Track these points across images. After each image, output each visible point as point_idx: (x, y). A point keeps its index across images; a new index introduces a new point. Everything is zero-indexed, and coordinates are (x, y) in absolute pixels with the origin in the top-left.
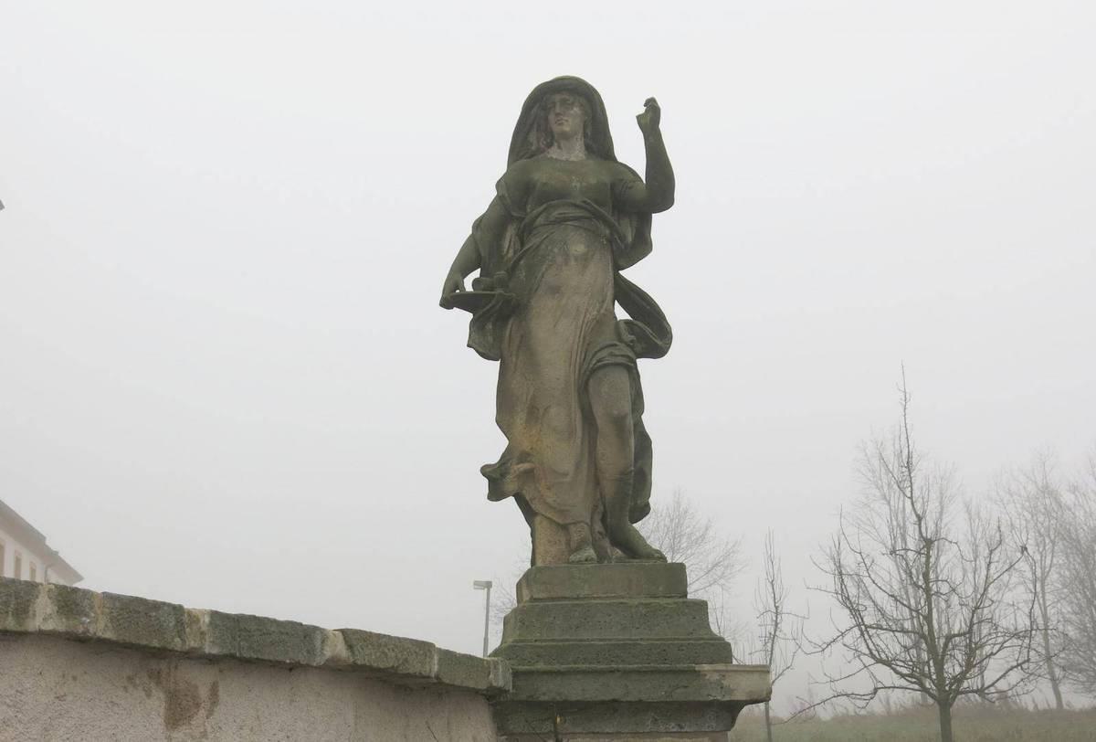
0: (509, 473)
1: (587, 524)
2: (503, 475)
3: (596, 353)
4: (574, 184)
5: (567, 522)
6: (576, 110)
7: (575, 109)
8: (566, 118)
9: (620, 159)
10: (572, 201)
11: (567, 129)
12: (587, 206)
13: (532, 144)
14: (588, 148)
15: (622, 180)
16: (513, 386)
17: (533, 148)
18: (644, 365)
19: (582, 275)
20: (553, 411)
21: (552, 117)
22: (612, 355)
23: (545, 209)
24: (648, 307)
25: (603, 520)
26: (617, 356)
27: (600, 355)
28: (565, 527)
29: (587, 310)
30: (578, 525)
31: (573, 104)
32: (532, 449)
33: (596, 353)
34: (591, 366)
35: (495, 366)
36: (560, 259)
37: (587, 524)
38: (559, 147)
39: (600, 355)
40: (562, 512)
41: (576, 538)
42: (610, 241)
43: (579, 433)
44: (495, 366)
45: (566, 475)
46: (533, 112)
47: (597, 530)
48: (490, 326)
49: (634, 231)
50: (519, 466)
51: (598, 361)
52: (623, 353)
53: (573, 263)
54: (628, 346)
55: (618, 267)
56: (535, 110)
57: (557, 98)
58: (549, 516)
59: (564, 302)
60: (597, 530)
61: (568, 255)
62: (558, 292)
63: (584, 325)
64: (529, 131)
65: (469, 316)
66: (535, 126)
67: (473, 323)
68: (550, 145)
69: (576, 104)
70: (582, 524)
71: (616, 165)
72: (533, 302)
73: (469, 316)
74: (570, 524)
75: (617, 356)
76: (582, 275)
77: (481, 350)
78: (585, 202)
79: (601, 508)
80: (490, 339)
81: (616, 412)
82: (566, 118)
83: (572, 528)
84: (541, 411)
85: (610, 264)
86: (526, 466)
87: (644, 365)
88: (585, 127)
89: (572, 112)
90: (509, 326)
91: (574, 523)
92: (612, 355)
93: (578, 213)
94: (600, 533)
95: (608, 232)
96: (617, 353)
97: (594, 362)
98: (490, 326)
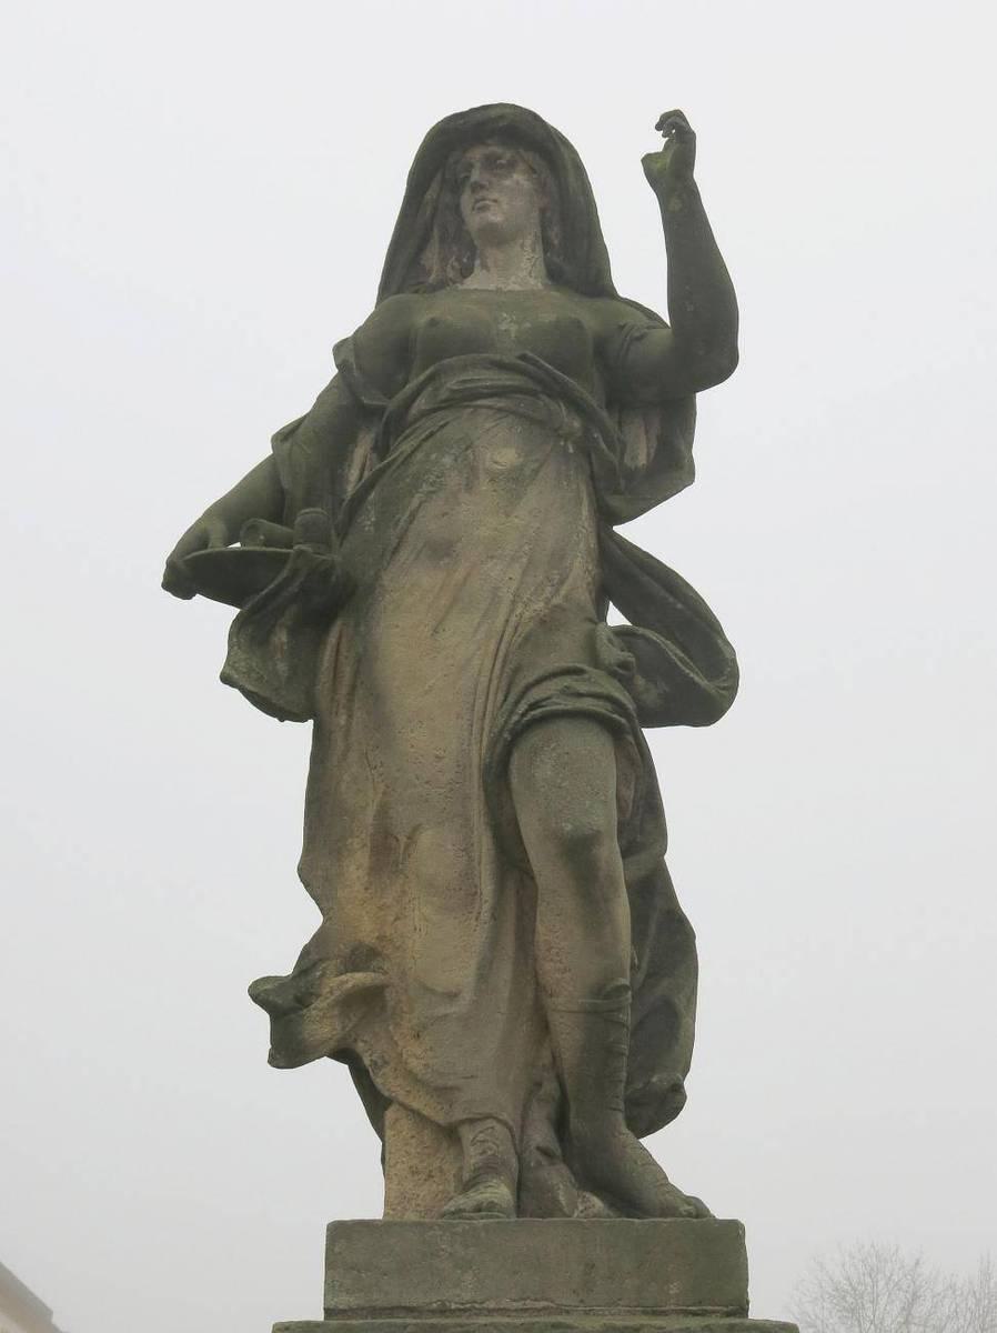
0: (318, 996)
1: (505, 1124)
3: (528, 688)
4: (503, 327)
5: (458, 1115)
6: (519, 178)
7: (515, 176)
8: (495, 195)
9: (622, 292)
10: (491, 356)
11: (495, 217)
12: (531, 367)
13: (429, 273)
14: (555, 276)
15: (622, 327)
16: (343, 787)
17: (432, 279)
19: (508, 515)
20: (426, 838)
21: (467, 200)
23: (431, 378)
24: (679, 606)
26: (580, 695)
27: (535, 695)
28: (450, 1134)
29: (517, 595)
30: (480, 1126)
31: (511, 165)
32: (381, 938)
33: (528, 688)
34: (515, 718)
35: (301, 734)
36: (454, 480)
37: (505, 1124)
38: (484, 266)
39: (535, 695)
40: (443, 1092)
41: (473, 1157)
42: (586, 450)
43: (487, 887)
44: (301, 734)
45: (452, 996)
46: (428, 196)
47: (533, 1145)
48: (281, 637)
49: (654, 444)
50: (343, 977)
51: (533, 706)
52: (598, 690)
53: (484, 485)
54: (613, 674)
55: (607, 516)
56: (430, 195)
57: (477, 154)
58: (415, 1105)
59: (459, 576)
60: (533, 1145)
61: (473, 469)
62: (448, 555)
63: (510, 630)
64: (424, 242)
65: (228, 613)
66: (436, 233)
67: (239, 626)
68: (466, 272)
69: (521, 166)
70: (490, 1123)
71: (615, 302)
72: (386, 579)
73: (228, 613)
74: (463, 1122)
75: (580, 695)
76: (508, 515)
77: (250, 687)
78: (523, 357)
79: (550, 1087)
80: (282, 667)
81: (569, 827)
83: (467, 1134)
84: (403, 840)
85: (586, 502)
88: (544, 226)
89: (507, 182)
90: (332, 639)
91: (471, 1121)
93: (506, 379)
94: (545, 1152)
95: (577, 424)
96: (583, 688)
97: (522, 707)
98: (281, 637)
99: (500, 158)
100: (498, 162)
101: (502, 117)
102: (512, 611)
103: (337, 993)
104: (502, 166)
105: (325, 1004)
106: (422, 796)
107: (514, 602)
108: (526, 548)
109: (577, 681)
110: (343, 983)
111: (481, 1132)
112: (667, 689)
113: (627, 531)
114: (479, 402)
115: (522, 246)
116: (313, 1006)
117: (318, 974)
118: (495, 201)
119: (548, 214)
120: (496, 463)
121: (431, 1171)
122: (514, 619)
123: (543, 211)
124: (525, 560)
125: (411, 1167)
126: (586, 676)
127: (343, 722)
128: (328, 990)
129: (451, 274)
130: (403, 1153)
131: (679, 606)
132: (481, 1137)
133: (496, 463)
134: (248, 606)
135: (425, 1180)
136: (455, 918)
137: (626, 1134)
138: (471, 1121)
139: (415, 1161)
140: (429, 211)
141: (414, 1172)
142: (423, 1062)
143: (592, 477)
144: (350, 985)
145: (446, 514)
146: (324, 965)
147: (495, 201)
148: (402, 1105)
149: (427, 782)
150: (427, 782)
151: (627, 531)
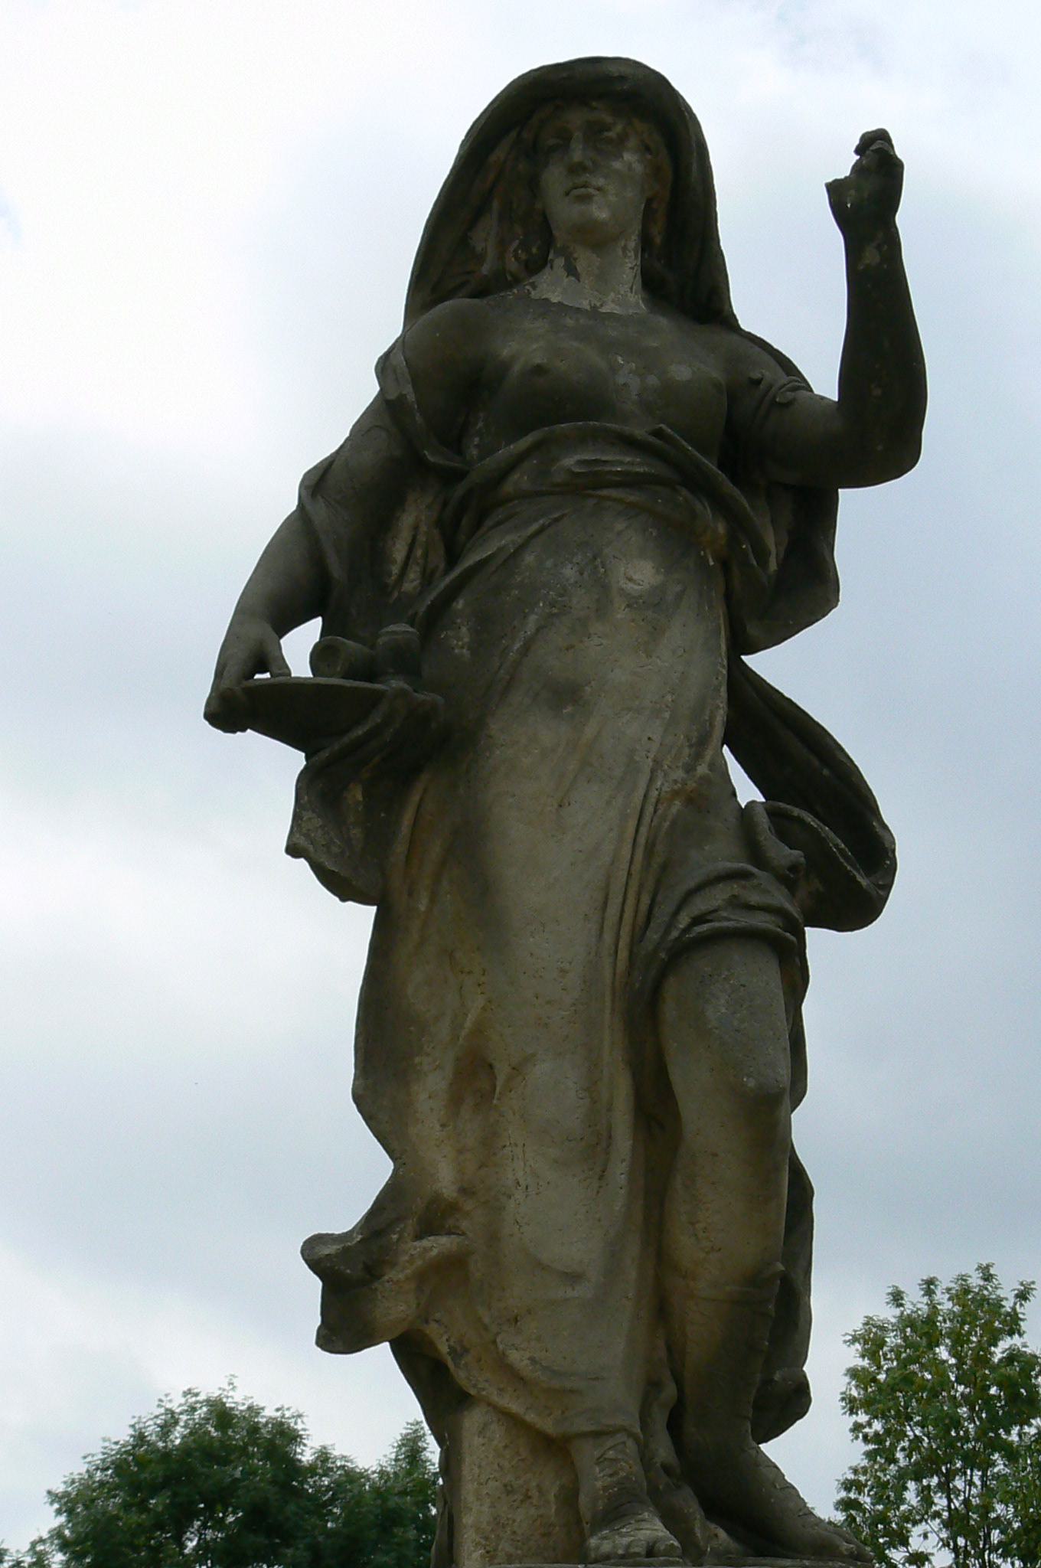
0: (393, 1265)
2: (373, 1272)
3: (691, 893)
4: (621, 380)
6: (630, 160)
7: (628, 156)
8: (601, 182)
9: (746, 323)
11: (600, 212)
13: (480, 259)
14: (652, 286)
15: (758, 382)
17: (486, 269)
18: (819, 942)
19: (649, 656)
20: (542, 1070)
21: (554, 178)
22: (738, 904)
23: (538, 446)
24: (826, 772)
25: (674, 1425)
26: (750, 908)
27: (700, 905)
29: (657, 763)
31: (622, 140)
33: (691, 893)
34: (675, 934)
35: (362, 917)
36: (581, 601)
38: (571, 271)
39: (700, 905)
41: (596, 1481)
44: (362, 917)
45: (573, 1278)
46: (493, 158)
47: (658, 1461)
48: (356, 794)
50: (426, 1243)
51: (698, 920)
52: (767, 900)
53: (621, 613)
55: (742, 642)
56: (499, 154)
57: (576, 119)
58: (515, 1407)
59: (590, 731)
60: (658, 1461)
61: (605, 588)
63: (650, 809)
64: (479, 212)
65: (294, 760)
66: (496, 205)
67: (306, 783)
68: (536, 266)
69: (632, 142)
71: (735, 337)
72: (494, 727)
73: (294, 760)
74: (584, 1435)
75: (750, 908)
76: (649, 656)
77: (330, 865)
78: (658, 434)
79: (670, 1391)
80: (356, 833)
81: (751, 1083)
82: (601, 182)
83: (586, 1454)
86: (438, 1245)
87: (819, 942)
89: (617, 165)
90: (415, 798)
91: (597, 1435)
92: (738, 904)
96: (754, 898)
97: (684, 921)
98: (356, 794)
99: (609, 129)
100: (606, 134)
101: (622, 78)
102: (651, 780)
103: (419, 1263)
104: (610, 141)
105: (401, 1276)
106: (540, 1019)
107: (653, 771)
108: (669, 698)
109: (744, 887)
110: (426, 1250)
111: (609, 1449)
112: (821, 889)
113: (755, 662)
114: (605, 492)
115: (625, 249)
116: (386, 1278)
117: (395, 1237)
118: (599, 189)
119: (655, 205)
120: (630, 580)
121: (528, 1490)
122: (654, 794)
123: (649, 202)
124: (667, 715)
125: (505, 1486)
126: (755, 881)
127: (422, 908)
128: (407, 1258)
129: (512, 265)
130: (496, 1466)
131: (826, 772)
132: (611, 1454)
133: (630, 580)
134: (324, 754)
135: (522, 1501)
136: (574, 1175)
137: (754, 1444)
138: (597, 1435)
139: (509, 1478)
140: (492, 176)
141: (509, 1489)
142: (528, 1355)
143: (728, 596)
144: (435, 1252)
145: (572, 647)
146: (402, 1226)
147: (599, 189)
148: (495, 1407)
149: (548, 1002)
150: (548, 1002)
151: (755, 662)
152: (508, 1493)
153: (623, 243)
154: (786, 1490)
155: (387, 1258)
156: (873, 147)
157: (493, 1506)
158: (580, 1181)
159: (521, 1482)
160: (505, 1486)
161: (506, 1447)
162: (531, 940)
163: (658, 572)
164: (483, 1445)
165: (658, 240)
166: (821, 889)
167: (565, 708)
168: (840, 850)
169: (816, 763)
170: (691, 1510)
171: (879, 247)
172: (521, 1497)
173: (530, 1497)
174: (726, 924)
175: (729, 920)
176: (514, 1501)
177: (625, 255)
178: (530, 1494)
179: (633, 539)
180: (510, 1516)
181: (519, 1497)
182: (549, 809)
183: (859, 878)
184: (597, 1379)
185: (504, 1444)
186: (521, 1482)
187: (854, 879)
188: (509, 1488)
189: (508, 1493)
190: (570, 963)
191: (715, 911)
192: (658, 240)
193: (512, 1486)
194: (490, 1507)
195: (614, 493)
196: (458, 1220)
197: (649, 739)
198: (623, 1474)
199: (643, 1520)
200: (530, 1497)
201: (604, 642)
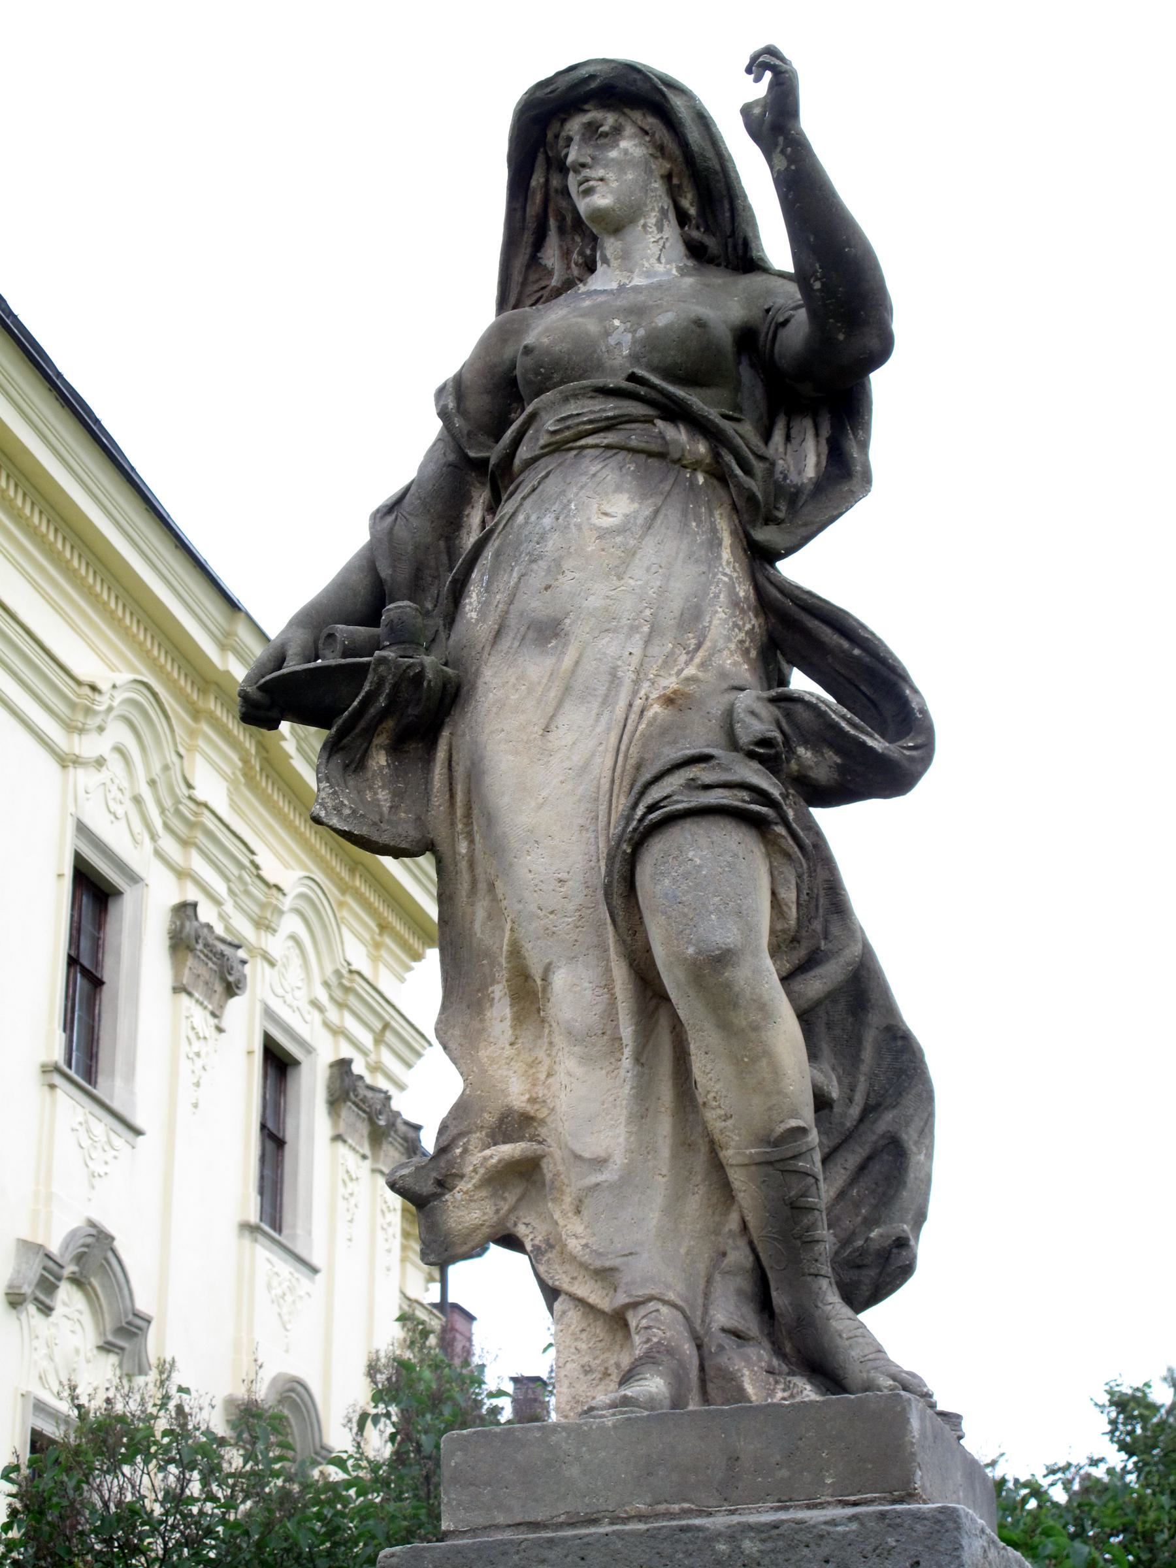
0: (462, 1176)
1: (674, 1306)
2: (444, 1185)
5: (622, 1299)
6: (629, 146)
7: (624, 144)
8: (601, 173)
10: (600, 381)
11: (602, 200)
12: (642, 391)
13: (550, 273)
14: (696, 252)
16: (477, 926)
17: (555, 282)
19: (620, 578)
20: (560, 979)
22: (693, 785)
24: (857, 652)
26: (707, 787)
27: (655, 794)
28: (618, 1321)
30: (642, 1311)
31: (617, 130)
32: (533, 1100)
37: (674, 1306)
39: (655, 794)
40: (605, 1275)
42: (719, 475)
43: (627, 1031)
45: (600, 1163)
46: (533, 183)
48: (380, 760)
49: (824, 449)
50: (488, 1152)
51: (651, 808)
54: (751, 755)
56: (537, 180)
57: (575, 125)
59: (568, 661)
60: (715, 1327)
62: (556, 635)
63: (633, 717)
66: (552, 223)
68: (590, 268)
69: (629, 130)
70: (652, 1305)
75: (707, 787)
76: (620, 578)
78: (632, 377)
81: (691, 951)
82: (601, 173)
84: (539, 982)
85: (727, 540)
86: (507, 1150)
88: (674, 193)
89: (613, 154)
92: (693, 785)
93: (611, 408)
94: (737, 1334)
95: (702, 448)
96: (708, 777)
97: (640, 811)
98: (380, 760)
99: (601, 125)
100: (601, 129)
101: (592, 77)
102: (635, 693)
103: (482, 1171)
104: (605, 135)
105: (470, 1186)
106: (547, 929)
107: (637, 682)
108: (648, 612)
109: (704, 769)
110: (485, 1159)
111: (643, 1317)
112: (839, 761)
113: (793, 569)
114: (582, 442)
115: (645, 226)
116: (457, 1189)
117: (458, 1151)
118: (602, 180)
119: (675, 181)
120: (606, 514)
121: (606, 1369)
122: (638, 703)
123: (668, 177)
124: (646, 629)
125: (583, 1366)
126: (714, 762)
127: (464, 851)
128: (471, 1168)
129: (576, 272)
130: (573, 1350)
131: (857, 652)
132: (644, 1323)
133: (606, 514)
134: (334, 729)
135: (601, 1379)
136: (601, 1068)
137: (832, 1301)
138: (635, 1305)
139: (586, 1359)
140: (538, 198)
141: (587, 1370)
142: (584, 1241)
143: (734, 507)
144: (494, 1161)
145: (550, 586)
146: (465, 1140)
147: (602, 180)
148: (566, 1294)
149: (552, 912)
150: (552, 912)
151: (793, 569)
152: (586, 1373)
153: (642, 222)
154: (856, 1339)
155: (454, 1171)
156: (761, 59)
157: (571, 1385)
158: (608, 1073)
159: (598, 1362)
160: (583, 1366)
161: (583, 1330)
162: (529, 858)
163: (632, 500)
164: (562, 1331)
165: (692, 211)
166: (839, 761)
167: (550, 643)
168: (843, 717)
169: (846, 645)
170: (736, 1368)
171: (783, 152)
172: (599, 1376)
173: (610, 1375)
174: (679, 806)
175: (682, 802)
176: (593, 1380)
177: (646, 232)
178: (609, 1372)
179: (609, 477)
180: (589, 1394)
181: (597, 1375)
182: (534, 736)
183: (870, 742)
184: (631, 1254)
185: (580, 1328)
186: (598, 1362)
187: (864, 744)
188: (588, 1369)
189: (586, 1373)
190: (569, 872)
191: (666, 798)
192: (692, 211)
193: (589, 1366)
194: (569, 1388)
195: (590, 440)
196: (536, 1129)
197: (630, 654)
198: (655, 1340)
199: (646, 1379)
200: (610, 1375)
201: (577, 575)
